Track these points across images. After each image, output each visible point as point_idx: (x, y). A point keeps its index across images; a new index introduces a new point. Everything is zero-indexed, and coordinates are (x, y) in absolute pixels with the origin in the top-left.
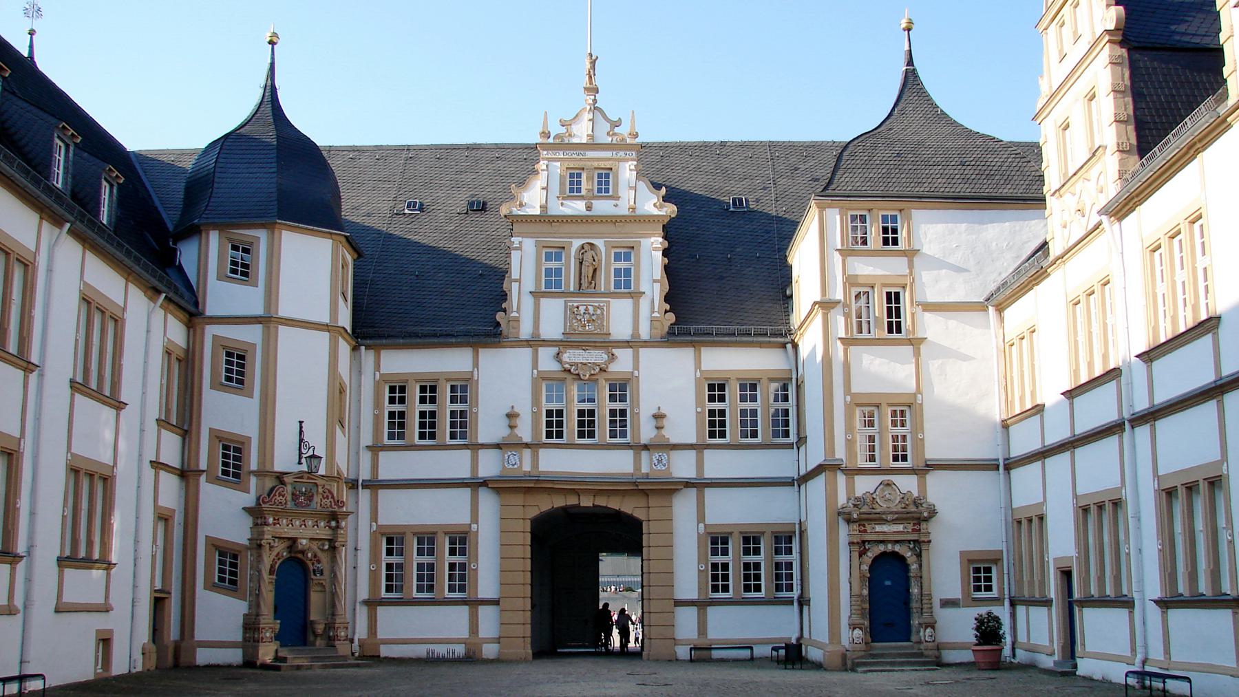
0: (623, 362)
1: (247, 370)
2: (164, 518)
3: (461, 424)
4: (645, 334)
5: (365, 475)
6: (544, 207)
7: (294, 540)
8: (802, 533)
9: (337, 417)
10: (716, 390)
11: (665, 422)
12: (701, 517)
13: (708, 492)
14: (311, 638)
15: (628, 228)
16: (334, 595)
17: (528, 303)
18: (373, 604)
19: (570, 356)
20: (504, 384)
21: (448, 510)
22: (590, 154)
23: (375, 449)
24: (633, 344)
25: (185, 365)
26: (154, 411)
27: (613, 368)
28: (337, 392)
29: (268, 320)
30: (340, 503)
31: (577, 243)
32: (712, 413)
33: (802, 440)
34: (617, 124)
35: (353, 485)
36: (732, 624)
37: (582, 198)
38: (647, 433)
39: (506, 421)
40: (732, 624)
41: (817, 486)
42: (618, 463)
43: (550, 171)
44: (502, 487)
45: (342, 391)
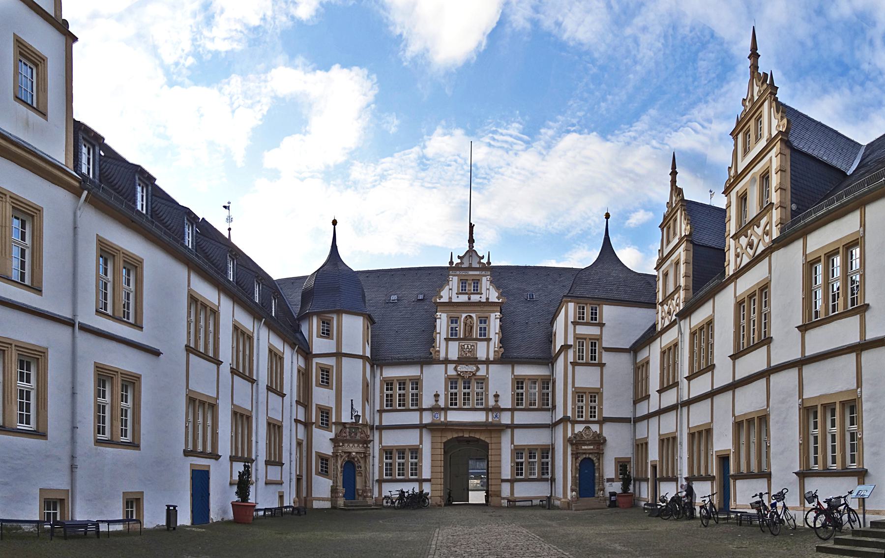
0: (482, 371)
1: (330, 377)
2: (299, 444)
3: (417, 399)
4: (491, 358)
5: (377, 423)
6: (450, 298)
7: (350, 453)
8: (553, 449)
9: (366, 398)
10: (519, 382)
11: (500, 399)
12: (512, 442)
13: (516, 431)
14: (357, 496)
15: (486, 308)
16: (366, 477)
17: (443, 343)
18: (380, 481)
19: (462, 368)
20: (434, 381)
21: (410, 439)
22: (471, 273)
23: (381, 411)
24: (487, 362)
25: (304, 375)
26: (295, 398)
27: (478, 374)
28: (366, 385)
29: (339, 355)
30: (368, 436)
31: (464, 315)
32: (518, 394)
33: (554, 407)
34: (483, 257)
35: (372, 428)
36: (523, 490)
37: (466, 294)
38: (491, 403)
39: (433, 399)
40: (523, 490)
41: (560, 429)
42: (479, 417)
43: (454, 282)
44: (432, 428)
45: (368, 386)
